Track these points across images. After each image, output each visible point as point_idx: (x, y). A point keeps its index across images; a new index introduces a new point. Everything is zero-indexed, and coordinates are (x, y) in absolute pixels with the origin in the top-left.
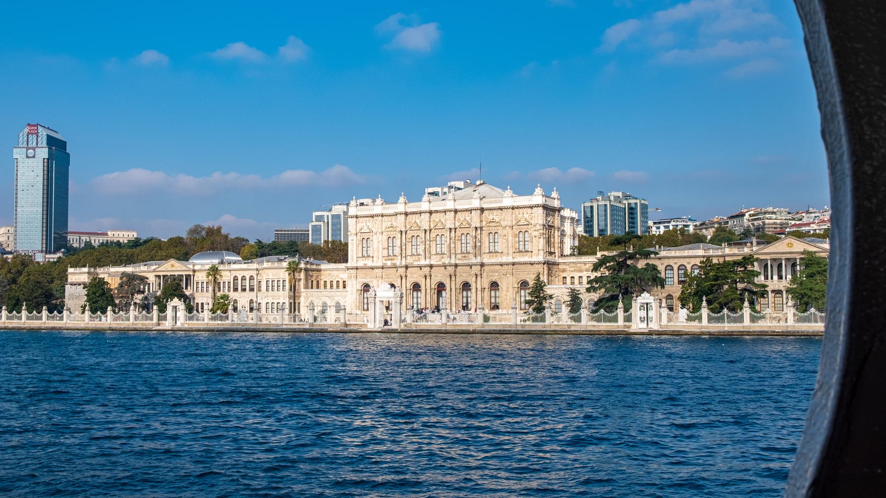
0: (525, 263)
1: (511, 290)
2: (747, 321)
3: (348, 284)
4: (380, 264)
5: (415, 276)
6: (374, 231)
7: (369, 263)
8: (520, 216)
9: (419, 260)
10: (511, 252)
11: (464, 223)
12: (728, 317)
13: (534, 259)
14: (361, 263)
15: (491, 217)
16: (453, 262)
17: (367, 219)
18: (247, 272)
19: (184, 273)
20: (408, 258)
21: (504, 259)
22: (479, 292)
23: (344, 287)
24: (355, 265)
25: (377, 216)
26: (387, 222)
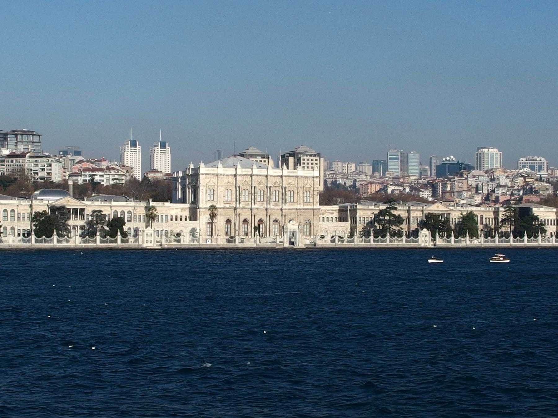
0: (310, 209)
2: (388, 242)
4: (222, 206)
5: (246, 214)
10: (302, 201)
11: (277, 184)
12: (45, 240)
16: (272, 207)
17: (212, 176)
18: (126, 208)
19: (79, 208)
21: (299, 207)
25: (221, 175)
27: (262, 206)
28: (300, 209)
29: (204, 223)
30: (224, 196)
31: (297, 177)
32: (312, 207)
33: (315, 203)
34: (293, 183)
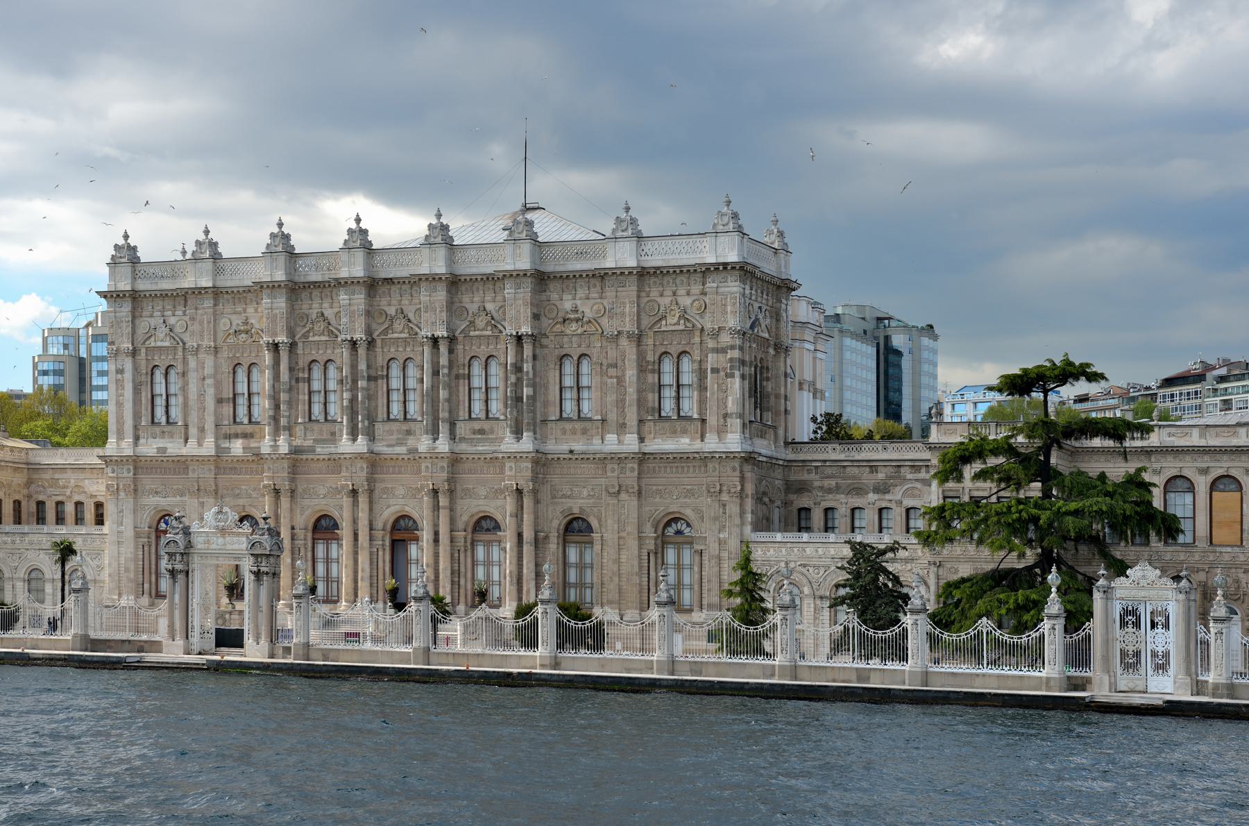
1: (633, 544)
3: (110, 511)
6: (192, 343)
7: (175, 447)
8: (665, 301)
9: (333, 438)
10: (632, 417)
11: (481, 322)
13: (712, 444)
14: (149, 448)
15: (568, 305)
20: (299, 430)
21: (611, 443)
22: (528, 550)
23: (100, 521)
24: (129, 452)
26: (231, 319)
27: (400, 443)
28: (619, 459)
29: (129, 533)
30: (220, 401)
31: (601, 276)
32: (698, 445)
33: (712, 420)
34: (588, 310)
